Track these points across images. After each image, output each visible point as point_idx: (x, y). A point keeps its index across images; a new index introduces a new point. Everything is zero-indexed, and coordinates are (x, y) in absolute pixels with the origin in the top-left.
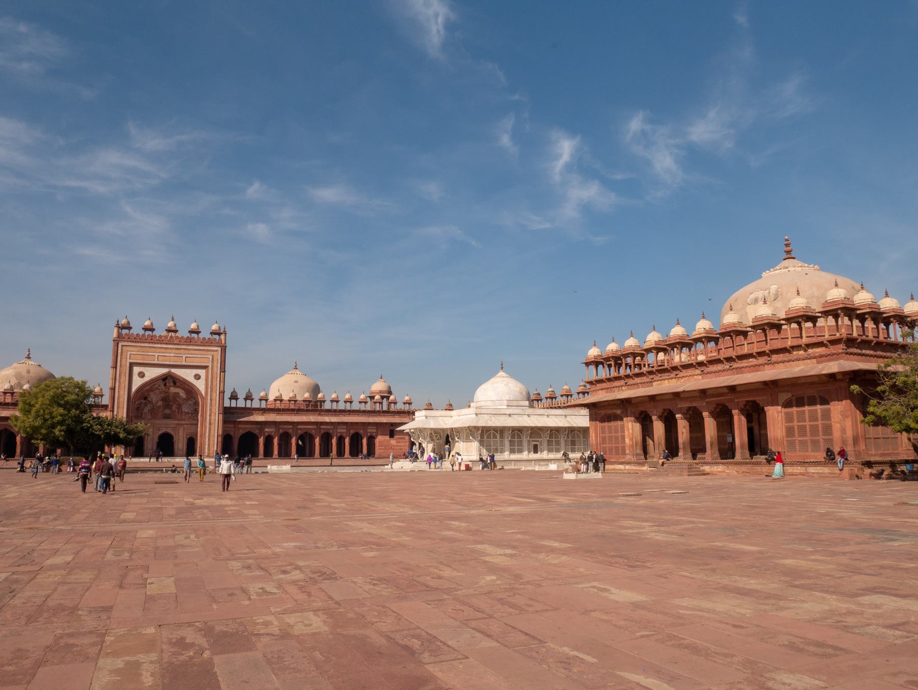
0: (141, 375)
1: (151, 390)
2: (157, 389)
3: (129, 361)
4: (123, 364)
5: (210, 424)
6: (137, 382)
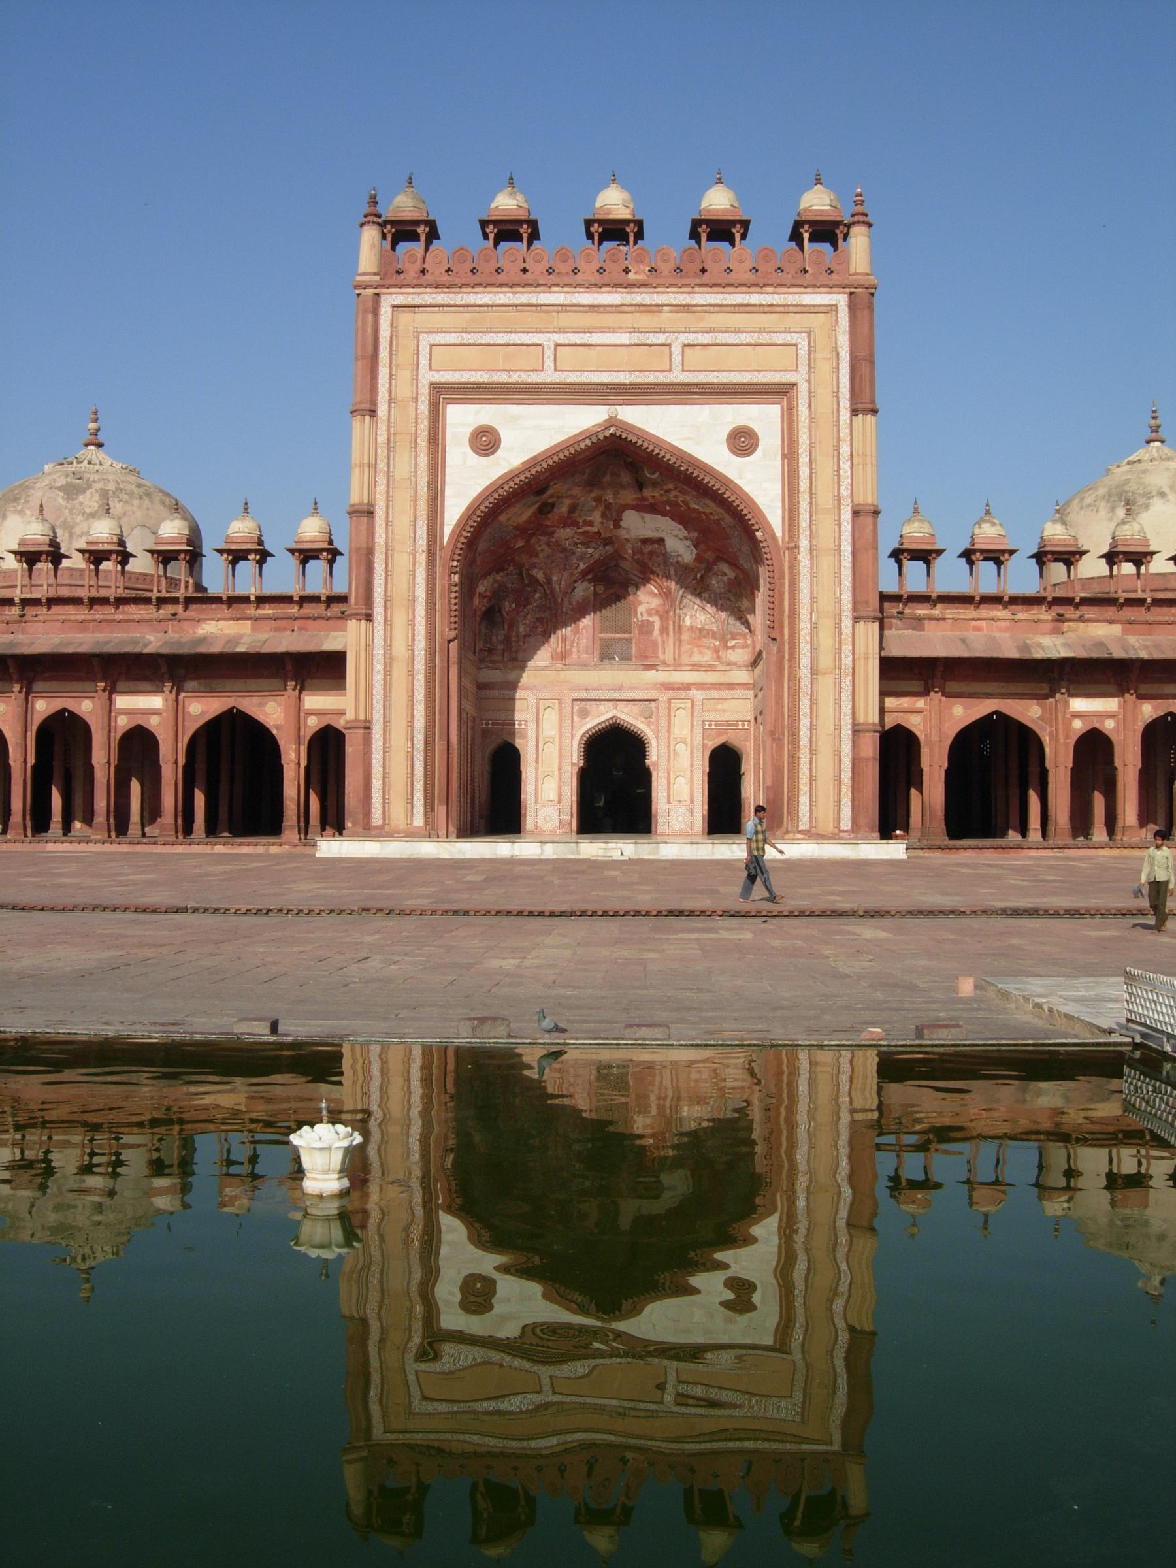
0: (485, 441)
1: (538, 526)
2: (568, 521)
3: (427, 377)
4: (404, 390)
5: (814, 672)
6: (468, 481)
